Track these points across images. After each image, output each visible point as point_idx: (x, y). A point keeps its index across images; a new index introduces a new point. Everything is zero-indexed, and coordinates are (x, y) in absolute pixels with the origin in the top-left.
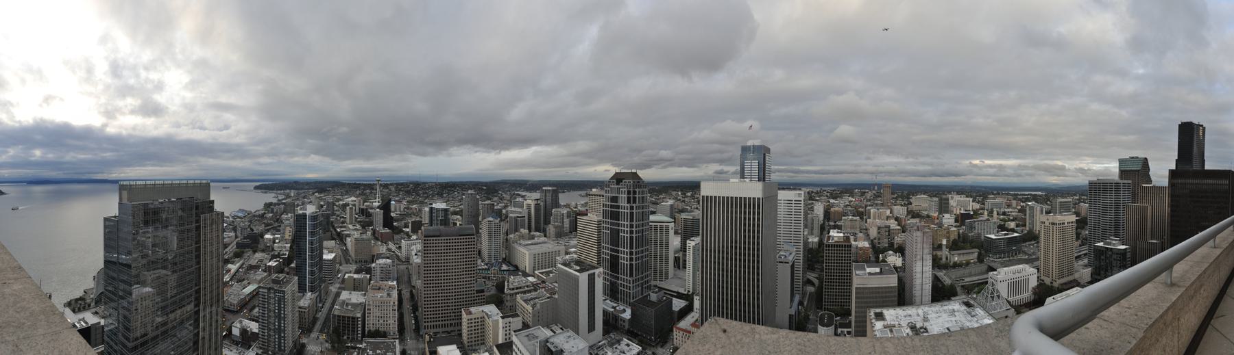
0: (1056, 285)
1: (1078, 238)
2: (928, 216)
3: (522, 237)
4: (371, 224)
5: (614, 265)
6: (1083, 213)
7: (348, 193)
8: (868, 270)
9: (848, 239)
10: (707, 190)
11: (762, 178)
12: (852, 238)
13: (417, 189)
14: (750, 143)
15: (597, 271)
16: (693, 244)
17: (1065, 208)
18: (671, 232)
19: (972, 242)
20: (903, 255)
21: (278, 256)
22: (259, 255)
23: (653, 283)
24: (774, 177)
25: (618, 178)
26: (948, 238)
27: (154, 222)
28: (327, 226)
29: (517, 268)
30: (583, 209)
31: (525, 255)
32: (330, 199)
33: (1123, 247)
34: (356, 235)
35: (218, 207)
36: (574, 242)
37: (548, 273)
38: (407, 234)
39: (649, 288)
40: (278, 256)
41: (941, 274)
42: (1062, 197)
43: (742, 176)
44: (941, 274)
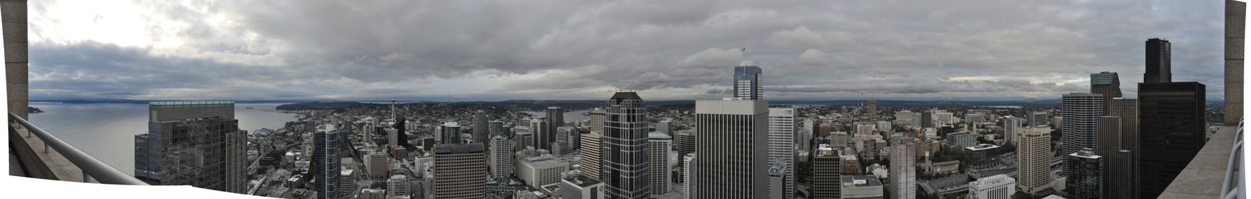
1: (1053, 149)
2: (912, 130)
3: (529, 154)
4: (386, 142)
5: (615, 179)
6: (1058, 126)
7: (364, 113)
8: (855, 182)
9: (836, 153)
10: (702, 108)
11: (754, 96)
12: (840, 152)
13: (430, 109)
14: (743, 64)
15: (599, 186)
16: (690, 159)
17: (1041, 121)
18: (669, 148)
19: (953, 153)
20: (888, 167)
21: (299, 172)
22: (281, 172)
25: (619, 98)
26: (931, 150)
27: (182, 140)
28: (345, 144)
29: (524, 183)
30: (586, 127)
31: (532, 170)
32: (348, 118)
34: (373, 152)
35: (241, 126)
36: (578, 158)
37: (553, 188)
38: (420, 151)
40: (299, 172)
41: (925, 184)
43: (736, 95)
44: (925, 184)
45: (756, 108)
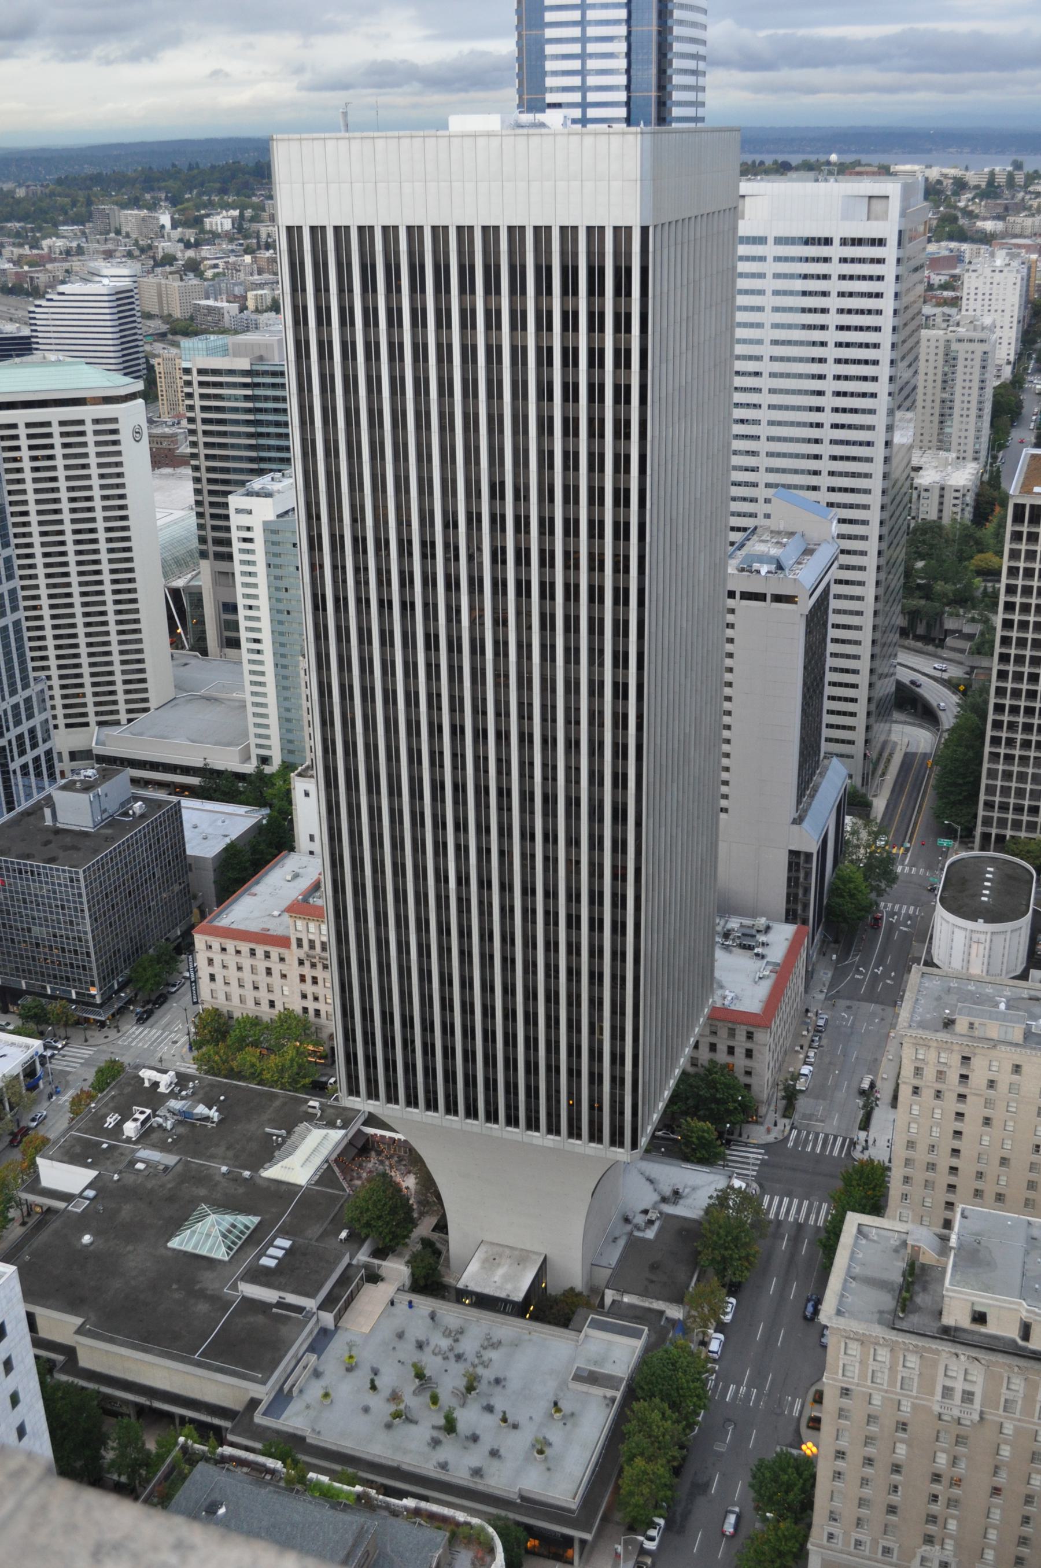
11: (653, 102)
16: (264, 511)
18: (136, 456)
23: (64, 741)
24: (723, 98)
39: (46, 767)
43: (533, 97)
45: (656, 177)
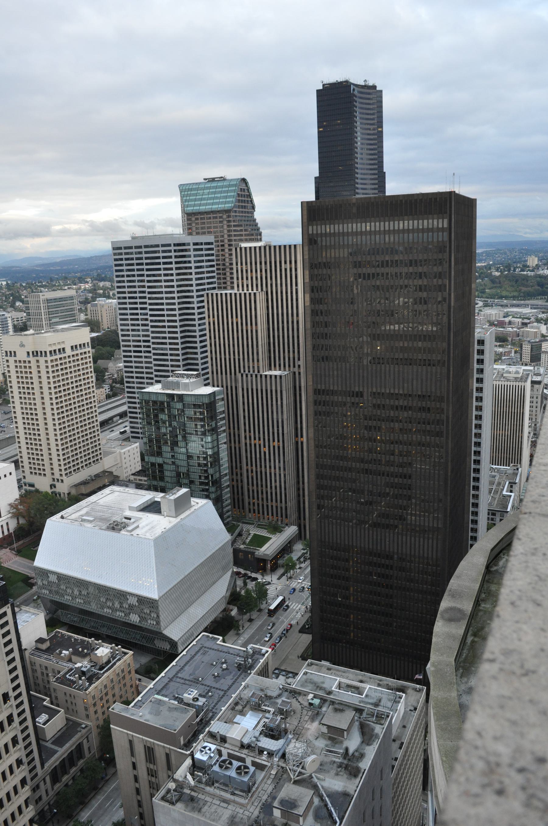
0: (63, 488)
1: (100, 380)
6: (106, 324)
17: (61, 313)
33: (208, 390)
42: (52, 287)
